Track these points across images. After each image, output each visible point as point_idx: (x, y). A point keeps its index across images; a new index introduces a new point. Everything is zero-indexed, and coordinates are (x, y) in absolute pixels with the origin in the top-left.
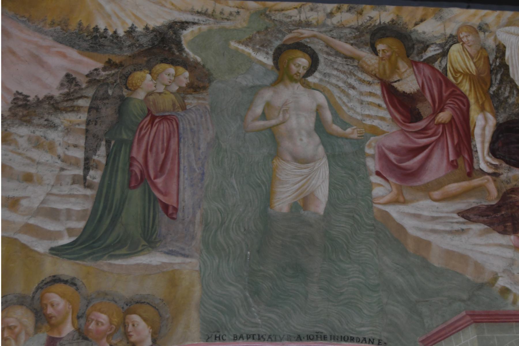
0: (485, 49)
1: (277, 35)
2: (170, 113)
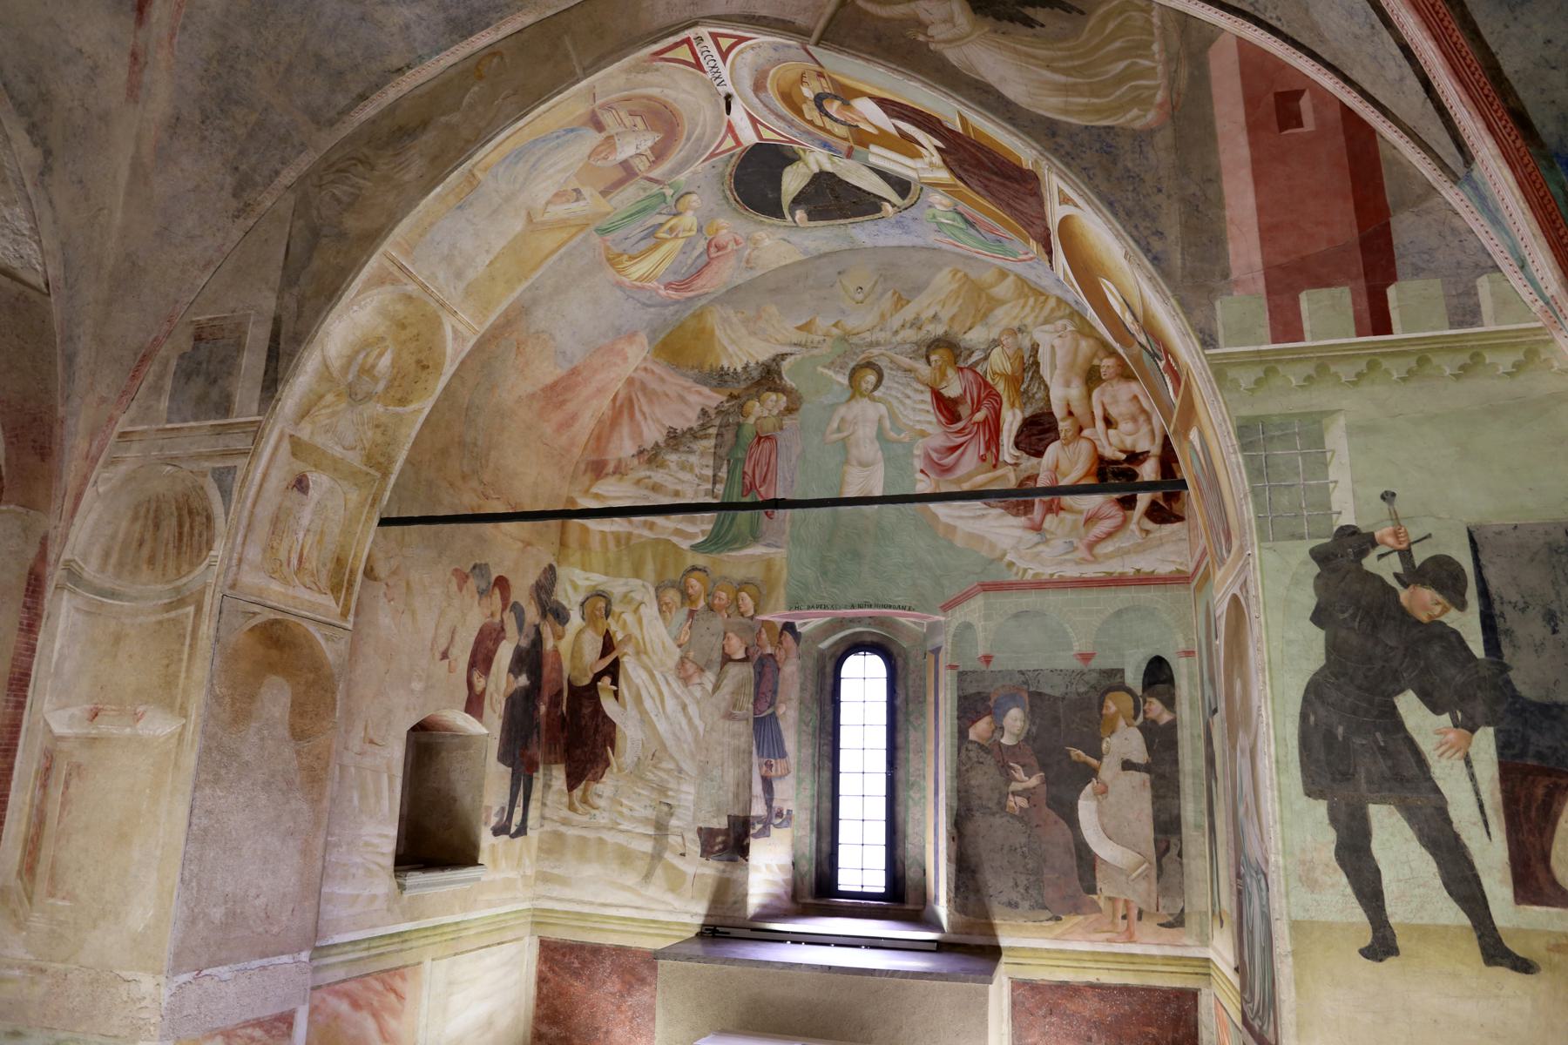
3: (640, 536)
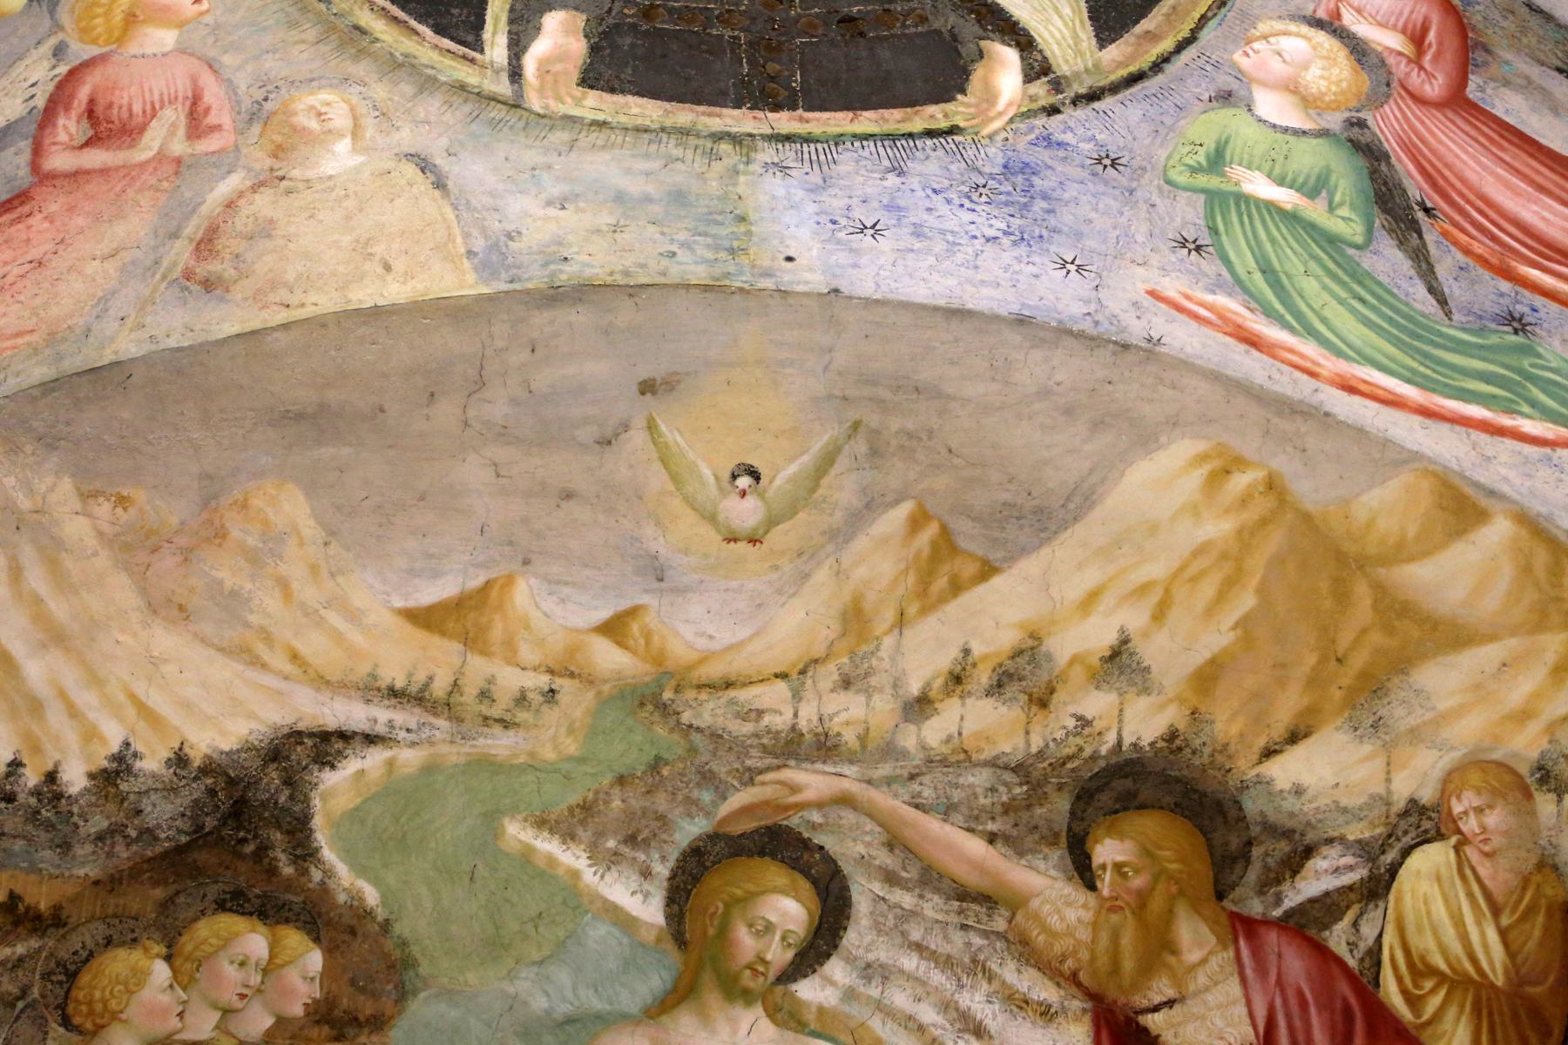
0: (1555, 868)
1: (695, 794)
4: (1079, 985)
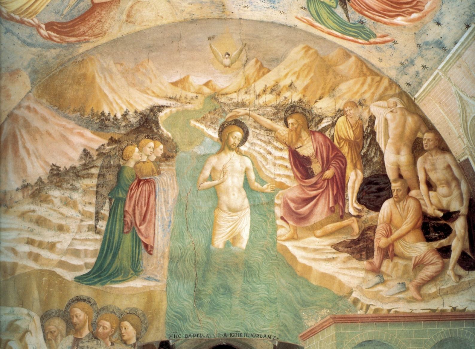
0: (361, 119)
2: (150, 177)
3: (25, 267)
4: (286, 144)
